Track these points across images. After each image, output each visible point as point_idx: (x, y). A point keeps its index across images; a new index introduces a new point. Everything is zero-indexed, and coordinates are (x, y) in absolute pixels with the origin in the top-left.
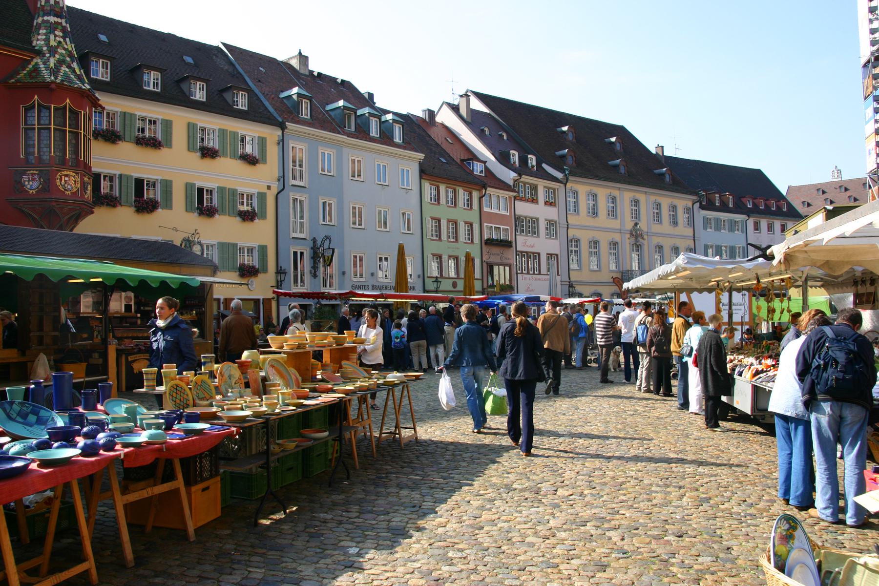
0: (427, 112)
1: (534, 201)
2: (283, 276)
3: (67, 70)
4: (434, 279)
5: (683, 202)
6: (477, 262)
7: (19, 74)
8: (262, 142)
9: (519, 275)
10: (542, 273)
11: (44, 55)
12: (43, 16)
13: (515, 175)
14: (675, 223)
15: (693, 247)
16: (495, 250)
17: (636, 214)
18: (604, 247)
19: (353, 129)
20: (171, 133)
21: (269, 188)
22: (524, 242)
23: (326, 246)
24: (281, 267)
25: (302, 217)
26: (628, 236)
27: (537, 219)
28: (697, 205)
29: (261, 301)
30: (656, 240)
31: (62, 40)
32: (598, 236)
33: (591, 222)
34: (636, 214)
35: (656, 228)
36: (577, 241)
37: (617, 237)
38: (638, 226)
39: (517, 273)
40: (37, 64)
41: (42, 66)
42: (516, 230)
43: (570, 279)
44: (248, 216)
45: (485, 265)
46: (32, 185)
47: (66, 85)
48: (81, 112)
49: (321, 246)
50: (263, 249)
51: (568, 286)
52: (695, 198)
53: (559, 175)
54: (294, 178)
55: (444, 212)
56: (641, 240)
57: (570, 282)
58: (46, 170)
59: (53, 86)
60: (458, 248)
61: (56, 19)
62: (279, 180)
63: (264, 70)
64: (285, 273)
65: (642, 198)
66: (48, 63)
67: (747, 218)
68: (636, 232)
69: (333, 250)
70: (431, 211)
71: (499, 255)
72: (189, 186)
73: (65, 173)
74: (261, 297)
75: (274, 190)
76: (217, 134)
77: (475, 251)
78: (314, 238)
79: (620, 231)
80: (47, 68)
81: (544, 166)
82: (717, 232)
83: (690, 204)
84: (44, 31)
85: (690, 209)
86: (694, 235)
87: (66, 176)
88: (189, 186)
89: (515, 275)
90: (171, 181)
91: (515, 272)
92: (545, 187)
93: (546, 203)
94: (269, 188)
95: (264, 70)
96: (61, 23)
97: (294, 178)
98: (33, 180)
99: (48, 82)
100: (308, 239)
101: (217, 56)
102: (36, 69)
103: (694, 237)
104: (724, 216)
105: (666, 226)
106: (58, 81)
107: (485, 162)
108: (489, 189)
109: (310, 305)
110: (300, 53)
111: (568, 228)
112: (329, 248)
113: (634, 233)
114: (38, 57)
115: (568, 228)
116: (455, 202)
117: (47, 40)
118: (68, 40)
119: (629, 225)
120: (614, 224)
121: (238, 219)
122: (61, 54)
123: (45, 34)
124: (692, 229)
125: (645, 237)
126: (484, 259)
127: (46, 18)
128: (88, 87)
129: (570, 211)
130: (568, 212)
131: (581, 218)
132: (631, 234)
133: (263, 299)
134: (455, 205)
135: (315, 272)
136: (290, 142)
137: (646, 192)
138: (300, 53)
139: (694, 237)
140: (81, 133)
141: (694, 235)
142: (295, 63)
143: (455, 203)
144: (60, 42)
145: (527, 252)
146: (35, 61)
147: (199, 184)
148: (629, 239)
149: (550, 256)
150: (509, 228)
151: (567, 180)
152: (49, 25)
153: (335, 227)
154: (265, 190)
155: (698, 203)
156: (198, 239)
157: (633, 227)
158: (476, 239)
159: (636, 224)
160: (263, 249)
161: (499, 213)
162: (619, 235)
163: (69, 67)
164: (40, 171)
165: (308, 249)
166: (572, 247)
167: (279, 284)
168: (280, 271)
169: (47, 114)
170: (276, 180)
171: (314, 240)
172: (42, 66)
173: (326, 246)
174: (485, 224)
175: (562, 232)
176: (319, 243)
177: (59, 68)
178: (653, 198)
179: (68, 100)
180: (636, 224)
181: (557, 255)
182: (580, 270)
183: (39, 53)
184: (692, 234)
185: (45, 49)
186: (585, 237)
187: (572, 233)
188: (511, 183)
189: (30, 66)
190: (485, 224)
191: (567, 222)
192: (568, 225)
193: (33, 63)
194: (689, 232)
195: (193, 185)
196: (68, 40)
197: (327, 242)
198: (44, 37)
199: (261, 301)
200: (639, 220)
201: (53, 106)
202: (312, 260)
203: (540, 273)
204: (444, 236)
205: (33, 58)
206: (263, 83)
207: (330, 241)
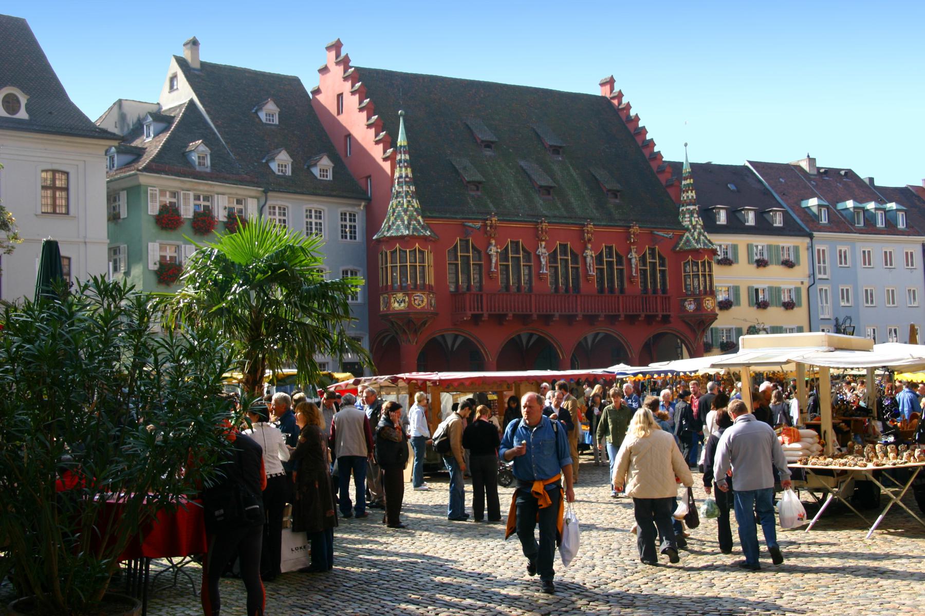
7: (679, 244)
8: (796, 249)
11: (690, 231)
12: (686, 206)
19: (862, 224)
20: (738, 253)
21: (802, 283)
23: (847, 325)
40: (687, 236)
41: (691, 238)
44: (789, 306)
46: (691, 307)
54: (820, 273)
62: (809, 277)
63: (783, 181)
69: (854, 327)
72: (749, 288)
73: (707, 299)
75: (806, 285)
80: (694, 239)
87: (708, 300)
88: (749, 288)
90: (739, 287)
94: (802, 283)
95: (783, 181)
97: (820, 273)
98: (691, 304)
102: (688, 241)
110: (808, 156)
117: (691, 221)
121: (782, 308)
122: (699, 229)
123: (689, 217)
127: (688, 207)
136: (816, 246)
138: (808, 156)
142: (805, 165)
144: (697, 221)
147: (756, 286)
154: (799, 285)
164: (695, 299)
165: (833, 327)
171: (837, 320)
172: (691, 238)
173: (847, 325)
176: (841, 321)
183: (687, 230)
185: (690, 226)
189: (684, 238)
193: (685, 236)
197: (848, 321)
198: (688, 219)
205: (684, 233)
206: (787, 195)
207: (851, 320)
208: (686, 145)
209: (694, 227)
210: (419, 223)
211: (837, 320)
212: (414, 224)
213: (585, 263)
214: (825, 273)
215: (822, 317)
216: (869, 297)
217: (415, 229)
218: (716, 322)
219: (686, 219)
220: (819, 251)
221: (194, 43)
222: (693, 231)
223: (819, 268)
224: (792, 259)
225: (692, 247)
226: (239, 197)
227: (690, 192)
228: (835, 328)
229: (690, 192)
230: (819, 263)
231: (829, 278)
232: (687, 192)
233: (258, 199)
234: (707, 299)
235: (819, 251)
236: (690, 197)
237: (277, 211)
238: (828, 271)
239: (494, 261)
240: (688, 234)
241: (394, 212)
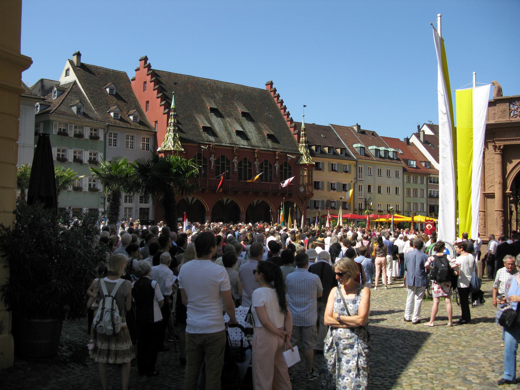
0: (406, 140)
6: (425, 205)
8: (350, 166)
45: (428, 206)
70: (407, 186)
72: (328, 183)
77: (424, 200)
88: (328, 183)
94: (352, 182)
97: (359, 178)
110: (357, 124)
126: (428, 204)
134: (417, 183)
138: (357, 124)
143: (416, 182)
147: (332, 182)
158: (425, 196)
171: (365, 199)
176: (367, 200)
195: (330, 182)
204: (412, 195)
210: (179, 145)
211: (365, 199)
212: (176, 145)
213: (255, 167)
214: (362, 178)
215: (359, 197)
217: (177, 147)
218: (313, 197)
220: (359, 167)
221: (78, 55)
223: (359, 175)
224: (348, 170)
225: (304, 163)
226: (96, 128)
230: (359, 173)
233: (104, 129)
235: (359, 167)
237: (113, 135)
239: (212, 164)
241: (167, 139)
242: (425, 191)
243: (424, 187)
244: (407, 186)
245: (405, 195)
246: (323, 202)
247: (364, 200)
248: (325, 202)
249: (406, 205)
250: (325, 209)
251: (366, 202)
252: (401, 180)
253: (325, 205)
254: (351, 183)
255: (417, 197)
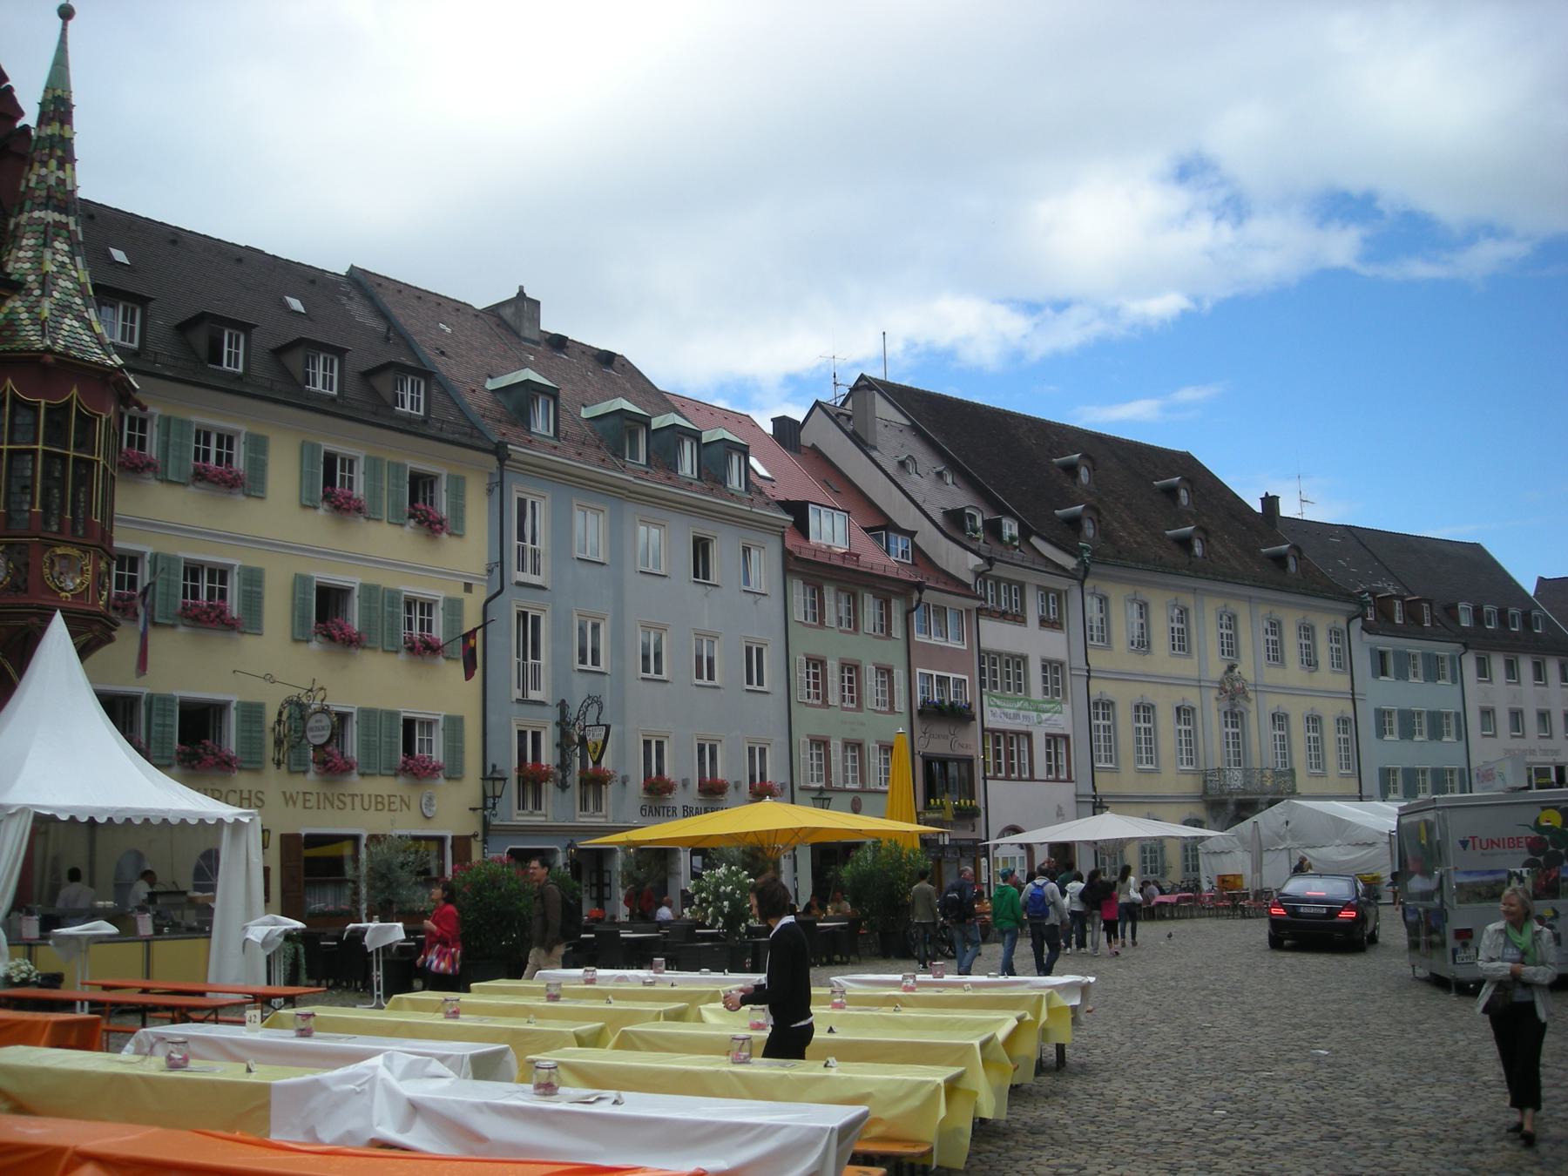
1: (1019, 618)
2: (499, 785)
3: (76, 324)
4: (815, 794)
5: (1325, 621)
9: (988, 781)
10: (1036, 778)
11: (29, 292)
13: (979, 561)
14: (1311, 663)
15: (1351, 715)
16: (940, 729)
17: (1230, 646)
18: (1166, 721)
21: (468, 588)
22: (998, 714)
23: (591, 720)
24: (494, 766)
25: (536, 655)
26: (1215, 693)
27: (1024, 658)
28: (1358, 623)
29: (449, 843)
30: (1273, 703)
31: (67, 260)
32: (1151, 694)
33: (1134, 663)
34: (1230, 646)
35: (1273, 675)
36: (1108, 705)
37: (1192, 697)
38: (1237, 670)
39: (985, 778)
40: (13, 311)
41: (24, 316)
42: (982, 684)
43: (1094, 789)
45: (919, 762)
47: (75, 357)
48: (100, 416)
49: (578, 719)
50: (455, 725)
51: (1091, 806)
52: (1352, 608)
53: (1069, 562)
55: (834, 645)
56: (1243, 702)
57: (1094, 797)
58: (22, 544)
59: (50, 358)
60: (863, 724)
61: (57, 216)
62: (490, 571)
63: (449, 330)
64: (504, 779)
65: (1242, 610)
66: (37, 310)
67: (1462, 650)
68: (1233, 686)
69: (608, 728)
70: (808, 642)
71: (947, 738)
74: (449, 833)
76: (362, 468)
77: (898, 728)
78: (563, 701)
79: (1199, 684)
81: (1034, 540)
82: (1402, 683)
83: (1341, 623)
84: (32, 242)
85: (1343, 631)
86: (1352, 689)
89: (982, 782)
91: (981, 775)
92: (1039, 587)
93: (1044, 622)
95: (449, 330)
96: (67, 224)
97: (521, 567)
99: (38, 350)
100: (549, 702)
101: (350, 299)
103: (1353, 694)
104: (1414, 646)
105: (1293, 672)
106: (58, 348)
107: (912, 534)
108: (926, 592)
109: (553, 852)
110: (521, 294)
111: (1089, 677)
112: (598, 725)
113: (1228, 688)
114: (17, 297)
115: (1089, 677)
116: (856, 621)
117: (38, 261)
118: (78, 259)
119: (1216, 669)
120: (1184, 667)
121: (402, 656)
122: (65, 291)
123: (31, 248)
124: (1349, 677)
125: (1251, 695)
127: (36, 214)
128: (120, 362)
129: (1092, 639)
130: (1089, 642)
131: (1116, 656)
132: (1222, 689)
133: (453, 837)
134: (856, 629)
135: (564, 777)
136: (514, 488)
137: (1250, 597)
138: (521, 294)
139: (1353, 694)
140: (98, 462)
141: (1352, 689)
144: (63, 265)
145: (1004, 732)
146: (10, 304)
148: (1217, 699)
149: (1052, 739)
150: (966, 677)
151: (1086, 573)
152: (41, 228)
153: (607, 677)
154: (459, 592)
155: (1360, 619)
156: (323, 700)
157: (1226, 673)
158: (901, 704)
159: (1231, 668)
160: (455, 725)
161: (946, 644)
162: (1196, 691)
163: (80, 318)
166: (1098, 719)
167: (488, 802)
168: (491, 777)
169: (29, 420)
170: (485, 572)
171: (563, 705)
172: (24, 316)
173: (591, 720)
174: (919, 670)
175: (1076, 686)
176: (573, 712)
177: (60, 319)
178: (1263, 610)
179: (75, 391)
180: (1231, 668)
181: (1066, 738)
182: (1115, 770)
183: (17, 287)
184: (1347, 688)
185: (31, 278)
186: (1124, 697)
187: (1099, 689)
188: (969, 579)
190: (919, 670)
191: (1088, 664)
192: (1088, 671)
194: (1341, 682)
196: (78, 259)
197: (593, 712)
198: (30, 254)
199: (449, 843)
200: (1238, 657)
201: (43, 402)
202: (558, 752)
203: (1032, 779)
204: (834, 698)
206: (449, 358)
207: (601, 708)
208: (66, 13)
209: (46, 282)
211: (563, 705)
214: (536, 570)
216: (651, 660)
219: (21, 254)
220: (522, 503)
222: (37, 292)
225: (20, 345)
227: (53, 163)
228: (558, 730)
229: (53, 163)
231: (548, 586)
232: (45, 164)
234: (59, 551)
235: (522, 503)
236: (52, 181)
238: (544, 564)
240: (18, 304)
242: (899, 675)
243: (892, 654)
244: (808, 642)
245: (799, 692)
246: (252, 713)
247: (552, 715)
248: (271, 717)
249: (804, 754)
250: (270, 768)
251: (563, 724)
252: (774, 605)
253: (270, 740)
254: (459, 592)
255: (860, 707)
